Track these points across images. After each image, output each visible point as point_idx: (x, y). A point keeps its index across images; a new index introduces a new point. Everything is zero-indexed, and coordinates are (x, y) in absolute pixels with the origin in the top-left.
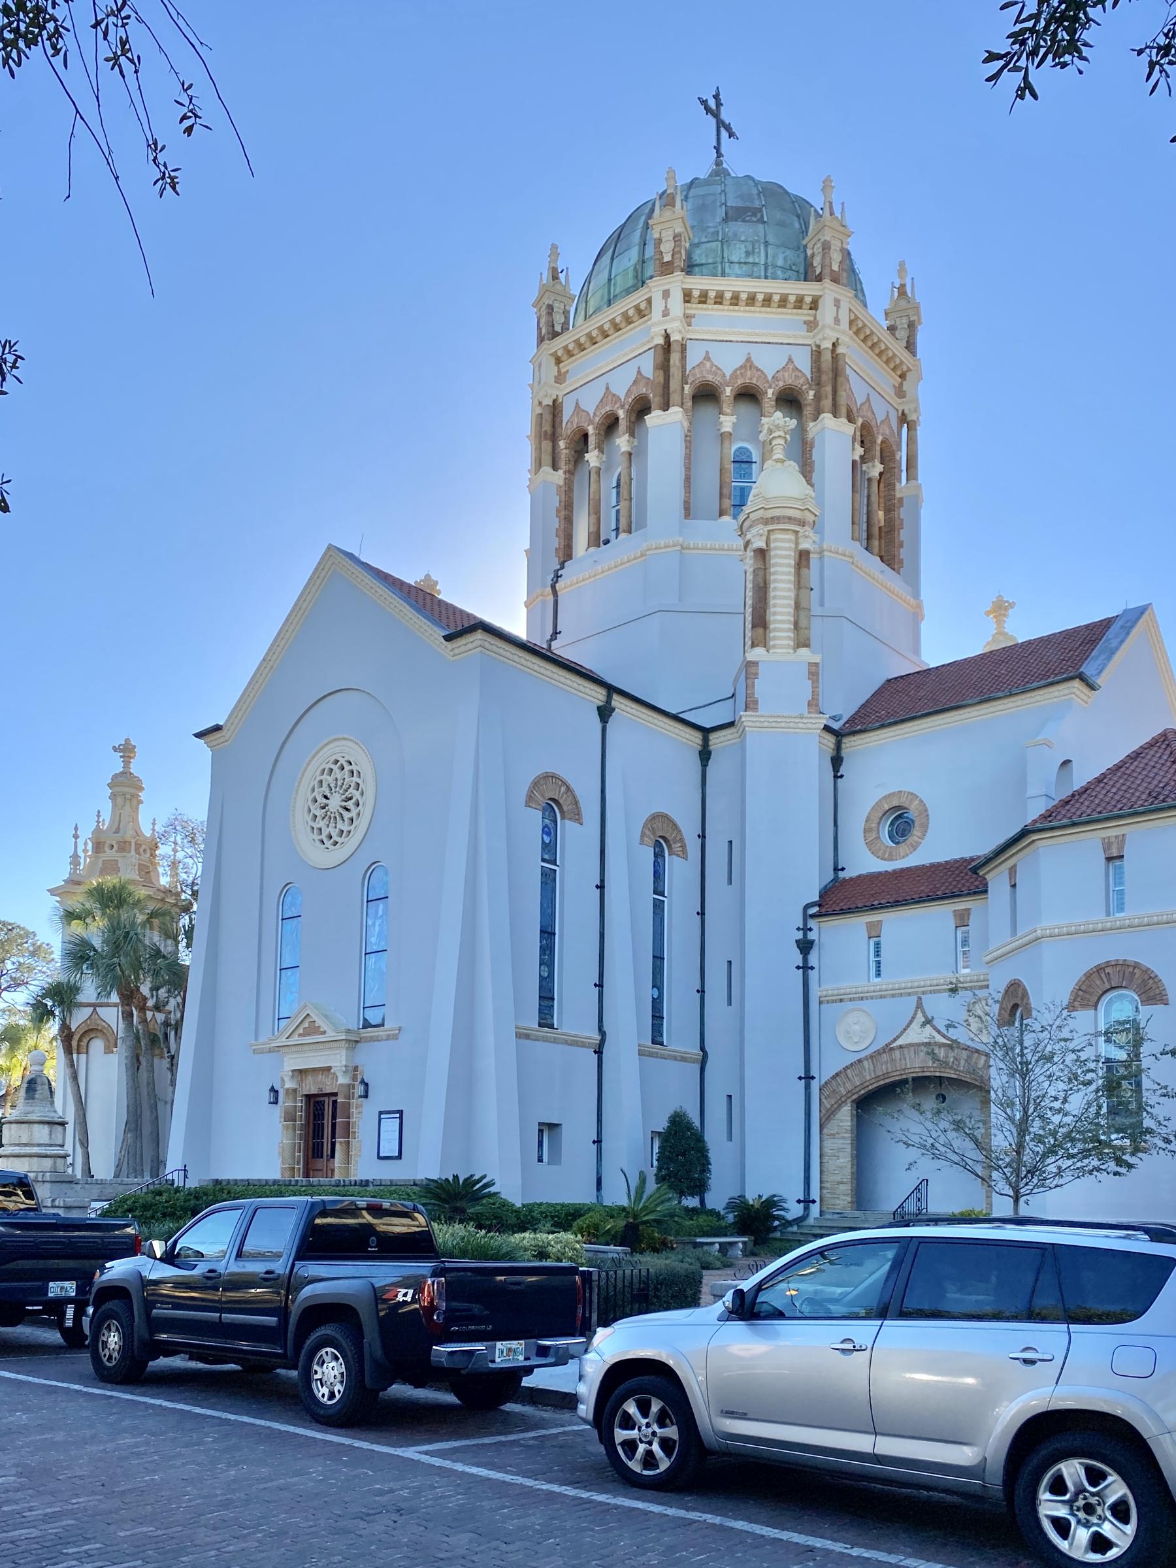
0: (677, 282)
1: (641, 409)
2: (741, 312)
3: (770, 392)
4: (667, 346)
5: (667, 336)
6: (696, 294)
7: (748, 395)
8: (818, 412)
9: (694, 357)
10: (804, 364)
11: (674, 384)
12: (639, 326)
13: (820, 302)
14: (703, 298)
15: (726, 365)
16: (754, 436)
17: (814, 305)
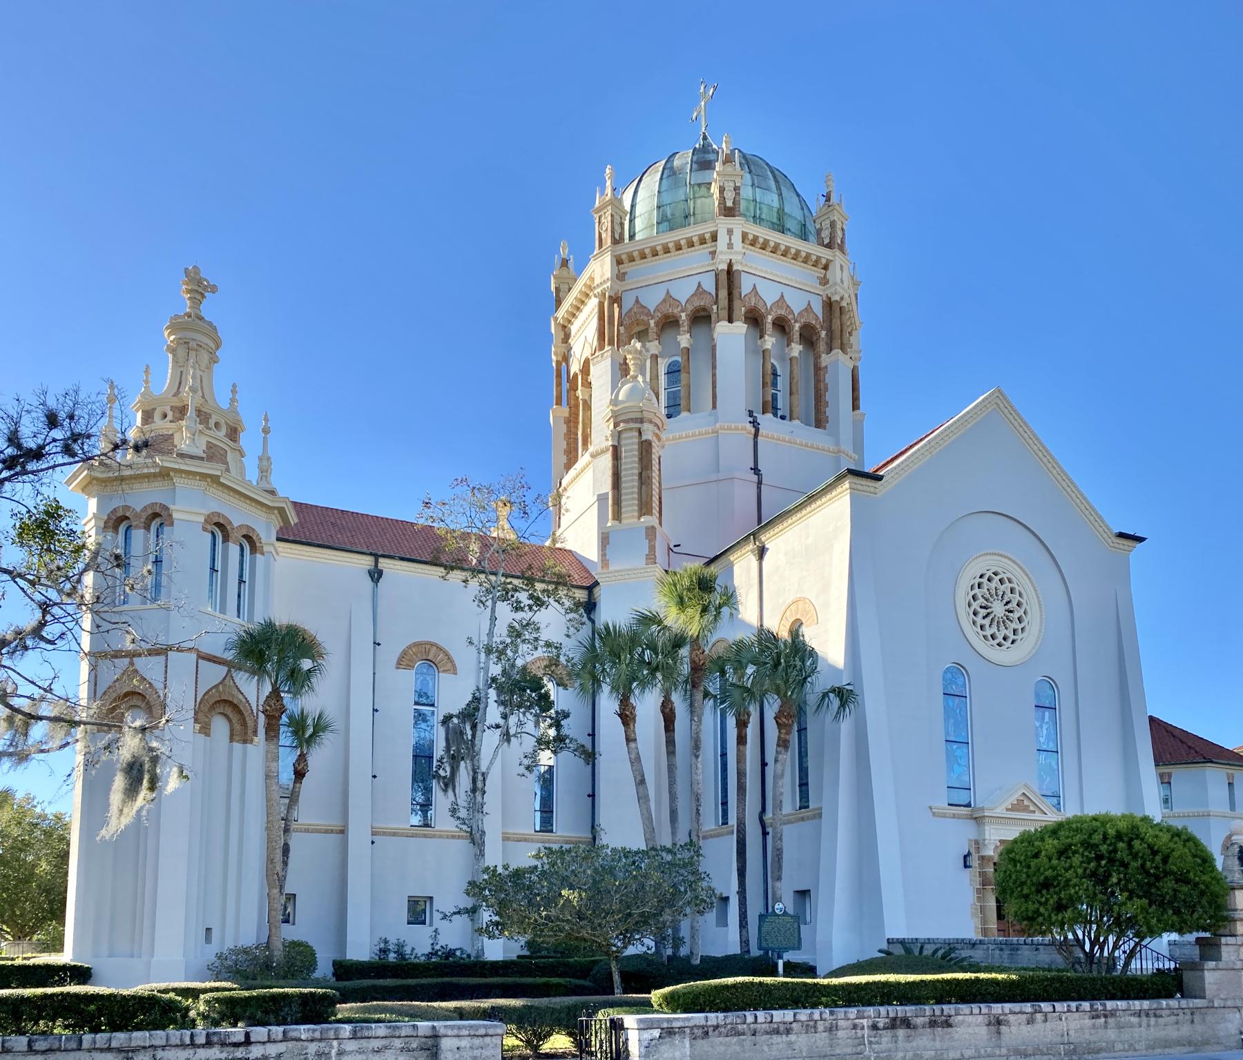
0: (738, 225)
1: (701, 318)
2: (777, 260)
3: (797, 326)
4: (730, 272)
5: (730, 265)
6: (751, 237)
7: (781, 326)
8: (830, 349)
9: (746, 285)
10: (818, 309)
11: (737, 303)
12: (701, 252)
13: (830, 267)
14: (753, 243)
15: (769, 296)
16: (782, 358)
17: (826, 268)
